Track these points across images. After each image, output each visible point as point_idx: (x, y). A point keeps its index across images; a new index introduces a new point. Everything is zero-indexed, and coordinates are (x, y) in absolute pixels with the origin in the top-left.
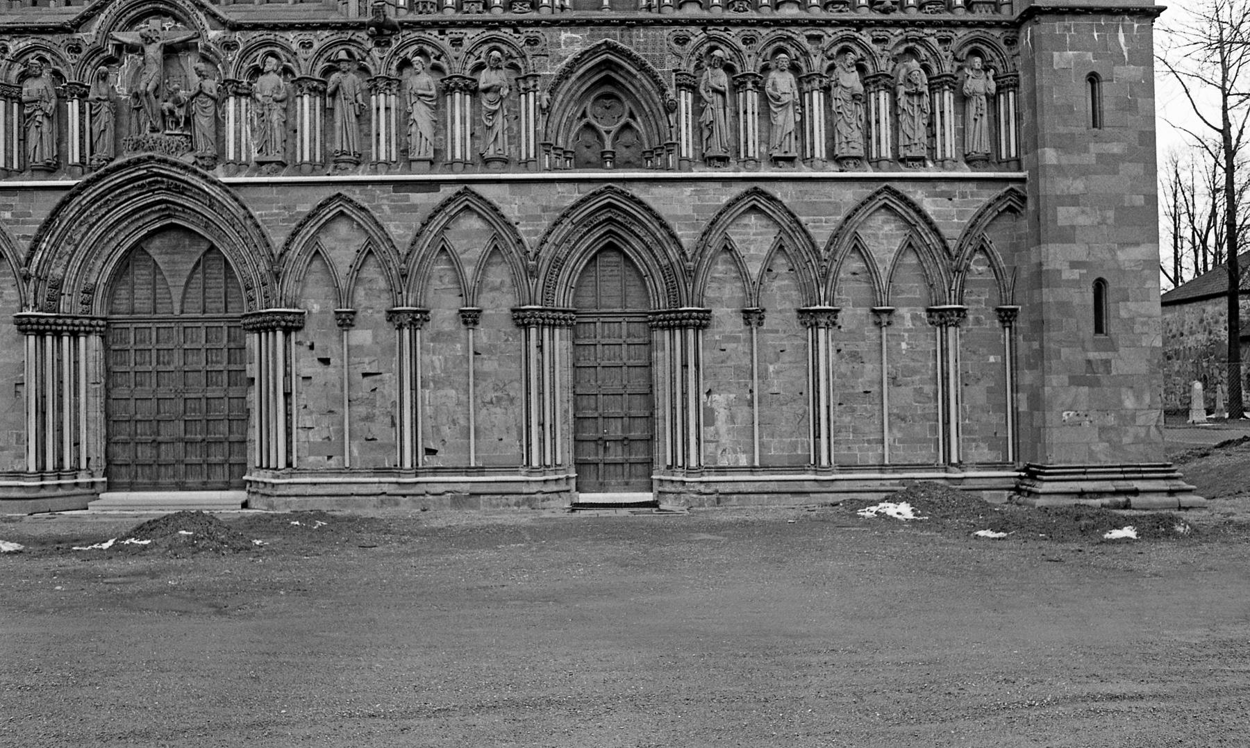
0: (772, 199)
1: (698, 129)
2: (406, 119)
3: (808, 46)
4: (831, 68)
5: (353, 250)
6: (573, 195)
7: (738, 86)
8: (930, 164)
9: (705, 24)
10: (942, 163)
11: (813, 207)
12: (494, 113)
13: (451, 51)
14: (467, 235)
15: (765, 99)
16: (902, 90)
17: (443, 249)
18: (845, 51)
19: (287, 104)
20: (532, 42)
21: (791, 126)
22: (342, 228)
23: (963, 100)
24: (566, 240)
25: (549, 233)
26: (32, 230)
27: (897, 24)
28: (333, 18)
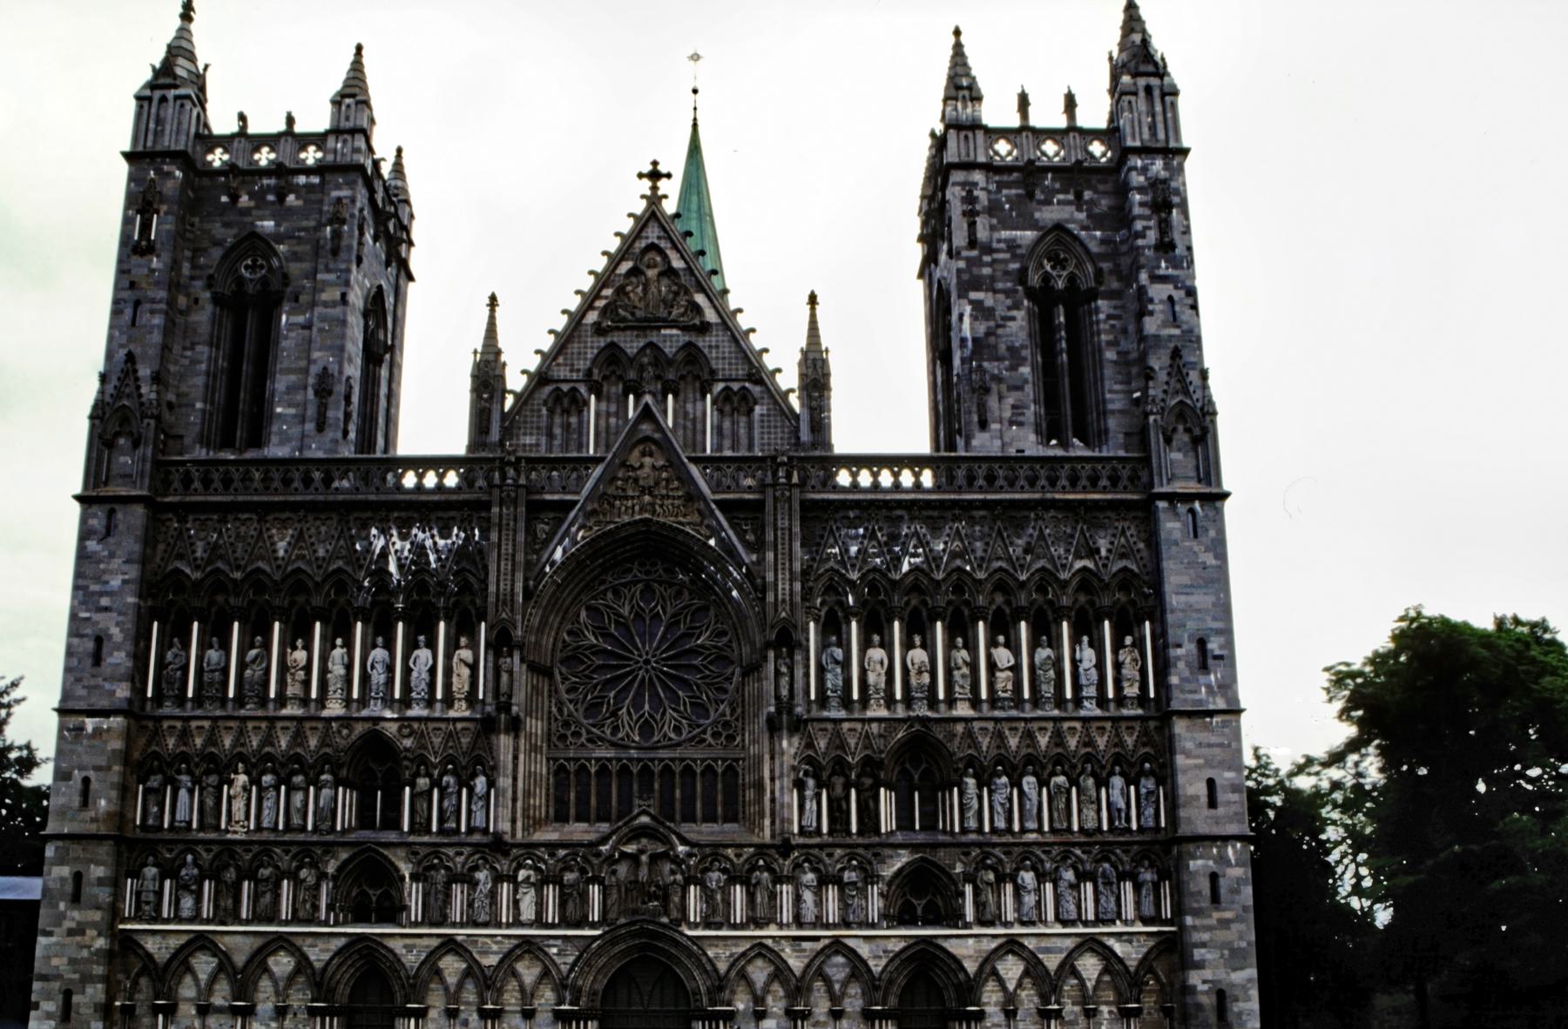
0: (1022, 946)
1: (977, 903)
2: (798, 899)
3: (1043, 856)
4: (1057, 869)
5: (766, 973)
6: (903, 944)
7: (1001, 879)
8: (1118, 922)
9: (979, 845)
10: (1126, 923)
11: (1048, 950)
12: (853, 897)
13: (827, 860)
14: (836, 965)
15: (1018, 891)
16: (1100, 881)
17: (821, 975)
18: (1064, 859)
19: (725, 891)
20: (876, 855)
21: (1033, 903)
22: (759, 962)
23: (1137, 888)
24: (896, 969)
25: (886, 966)
26: (571, 959)
27: (1096, 843)
28: (756, 840)
